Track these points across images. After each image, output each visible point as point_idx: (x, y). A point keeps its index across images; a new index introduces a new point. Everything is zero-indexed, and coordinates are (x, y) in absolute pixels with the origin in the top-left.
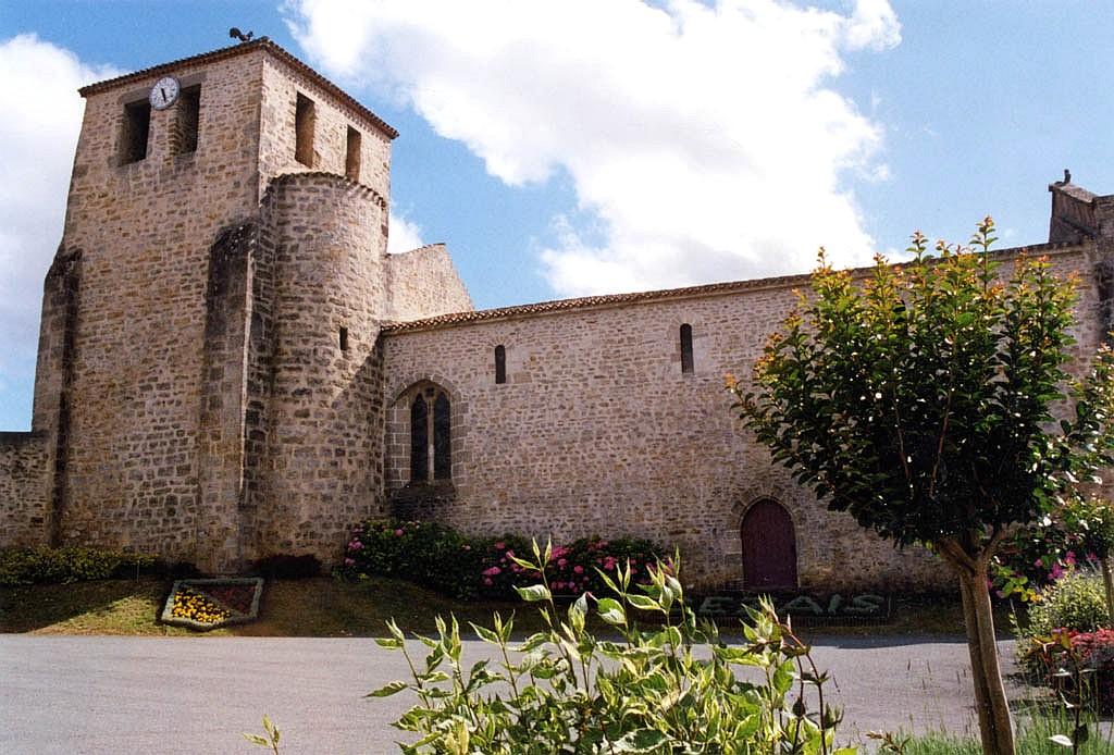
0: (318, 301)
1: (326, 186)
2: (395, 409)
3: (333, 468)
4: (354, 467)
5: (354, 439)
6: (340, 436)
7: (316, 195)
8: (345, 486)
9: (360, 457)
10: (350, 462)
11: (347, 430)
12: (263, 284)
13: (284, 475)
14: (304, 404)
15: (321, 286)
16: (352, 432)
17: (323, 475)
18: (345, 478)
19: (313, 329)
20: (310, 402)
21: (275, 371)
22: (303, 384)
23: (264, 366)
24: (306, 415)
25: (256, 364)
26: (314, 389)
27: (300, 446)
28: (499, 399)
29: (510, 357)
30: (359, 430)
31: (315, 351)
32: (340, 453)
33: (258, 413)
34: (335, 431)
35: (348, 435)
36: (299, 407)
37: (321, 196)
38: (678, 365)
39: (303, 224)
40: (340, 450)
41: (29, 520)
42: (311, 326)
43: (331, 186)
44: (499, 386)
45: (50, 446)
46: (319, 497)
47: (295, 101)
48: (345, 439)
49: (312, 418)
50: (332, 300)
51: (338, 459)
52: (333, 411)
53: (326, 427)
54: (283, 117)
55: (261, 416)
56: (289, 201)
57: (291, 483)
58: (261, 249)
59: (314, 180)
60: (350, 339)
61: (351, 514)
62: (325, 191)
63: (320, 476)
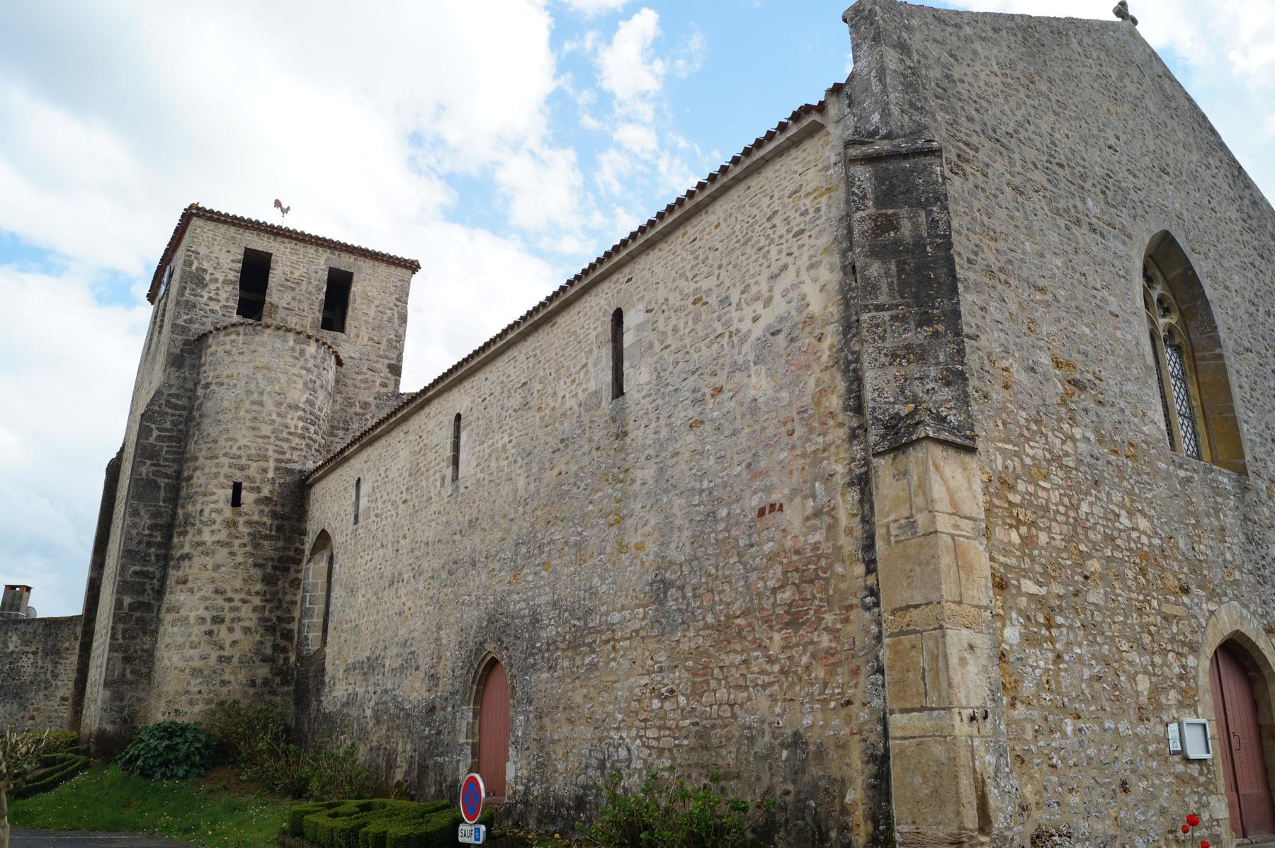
0: (211, 458)
1: (233, 337)
2: (312, 565)
3: (207, 638)
4: (238, 634)
5: (240, 604)
6: (219, 601)
7: (223, 347)
8: (220, 657)
9: (247, 624)
10: (231, 630)
11: (229, 594)
12: (165, 449)
13: (163, 647)
14: (184, 571)
15: (215, 442)
16: (237, 597)
17: (193, 646)
18: (222, 648)
19: (203, 489)
20: (190, 566)
21: (171, 537)
22: (187, 549)
23: (157, 534)
24: (185, 582)
25: (147, 532)
26: (195, 553)
27: (177, 616)
28: (353, 541)
29: (365, 488)
30: (249, 593)
31: (202, 511)
32: (218, 620)
33: (144, 584)
34: (214, 596)
35: (230, 600)
36: (180, 573)
37: (228, 347)
38: (449, 472)
39: (209, 380)
40: (217, 617)
41: (58, 699)
42: (200, 486)
43: (238, 334)
44: (355, 527)
45: (79, 630)
46: (187, 671)
47: (241, 257)
48: (227, 605)
49: (190, 585)
50: (225, 455)
51: (215, 628)
52: (214, 574)
53: (203, 593)
54: (220, 277)
55: (148, 586)
56: (203, 360)
57: (166, 655)
58: (167, 413)
59: (223, 333)
60: (244, 493)
61: (225, 690)
62: (233, 341)
63: (191, 647)
